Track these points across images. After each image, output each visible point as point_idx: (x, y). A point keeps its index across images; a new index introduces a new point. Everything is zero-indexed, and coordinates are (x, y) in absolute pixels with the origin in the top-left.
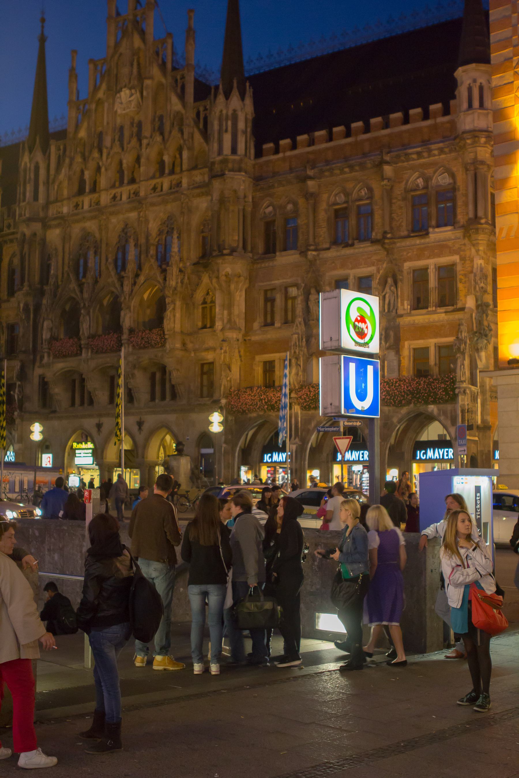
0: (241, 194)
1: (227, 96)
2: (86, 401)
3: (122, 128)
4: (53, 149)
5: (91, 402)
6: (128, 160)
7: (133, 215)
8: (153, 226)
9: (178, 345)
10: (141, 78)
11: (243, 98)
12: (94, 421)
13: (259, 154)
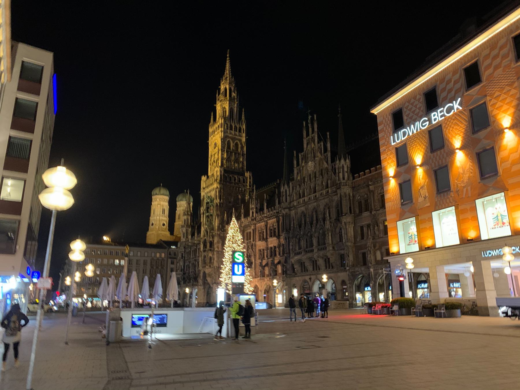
0: (347, 193)
1: (340, 160)
2: (303, 270)
3: (310, 175)
4: (291, 184)
5: (307, 271)
6: (312, 185)
7: (315, 204)
8: (322, 207)
9: (331, 248)
10: (314, 157)
11: (345, 160)
12: (309, 277)
13: (354, 179)
